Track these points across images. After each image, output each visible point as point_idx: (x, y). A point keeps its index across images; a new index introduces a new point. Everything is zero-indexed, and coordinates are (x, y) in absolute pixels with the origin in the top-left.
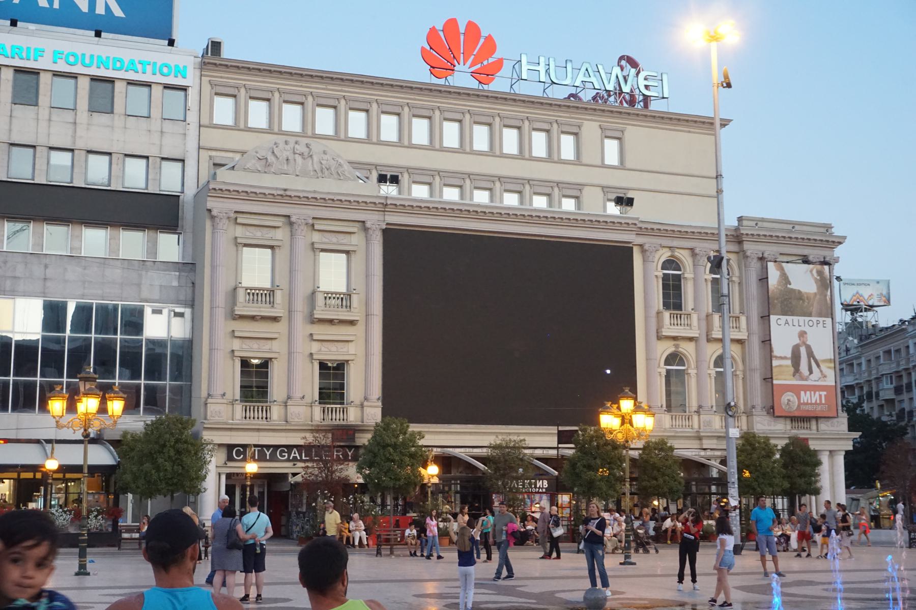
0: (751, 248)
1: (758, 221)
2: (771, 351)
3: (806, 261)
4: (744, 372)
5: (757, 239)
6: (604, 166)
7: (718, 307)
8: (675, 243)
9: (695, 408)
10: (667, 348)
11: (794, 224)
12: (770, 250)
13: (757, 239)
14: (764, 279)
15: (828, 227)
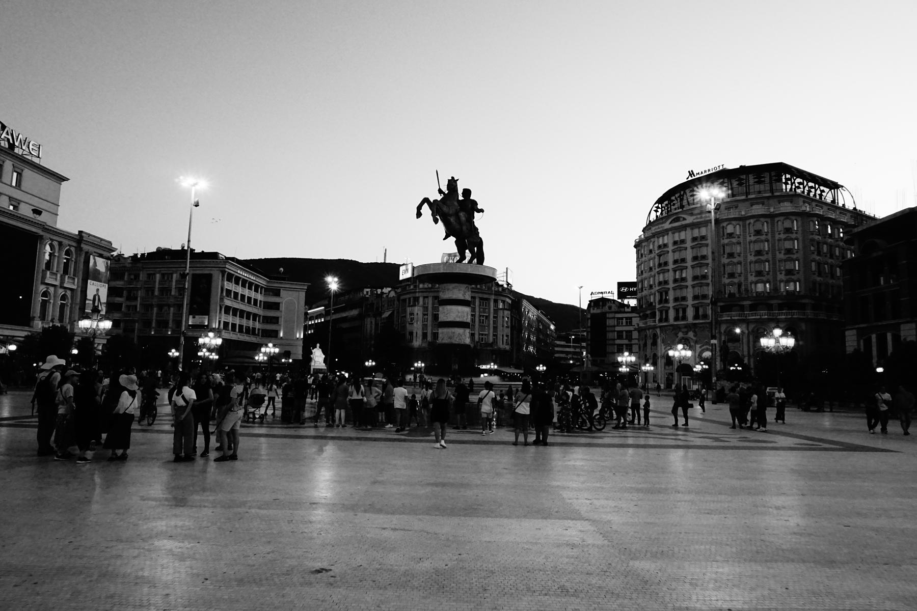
0: (85, 247)
1: (89, 235)
2: (86, 295)
3: (101, 256)
4: (71, 304)
5: (88, 243)
6: (11, 186)
7: (66, 271)
8: (55, 238)
9: (50, 318)
10: (42, 288)
11: (102, 240)
12: (91, 249)
13: (88, 243)
14: (87, 262)
15: (110, 243)
